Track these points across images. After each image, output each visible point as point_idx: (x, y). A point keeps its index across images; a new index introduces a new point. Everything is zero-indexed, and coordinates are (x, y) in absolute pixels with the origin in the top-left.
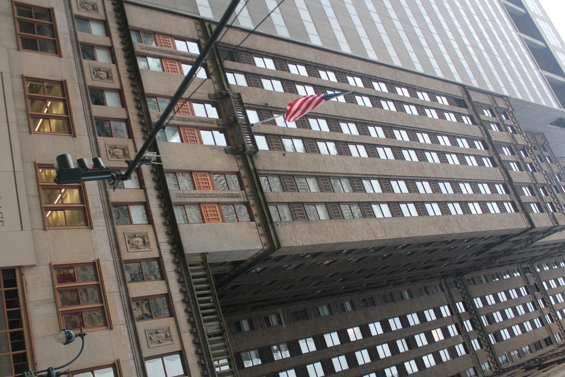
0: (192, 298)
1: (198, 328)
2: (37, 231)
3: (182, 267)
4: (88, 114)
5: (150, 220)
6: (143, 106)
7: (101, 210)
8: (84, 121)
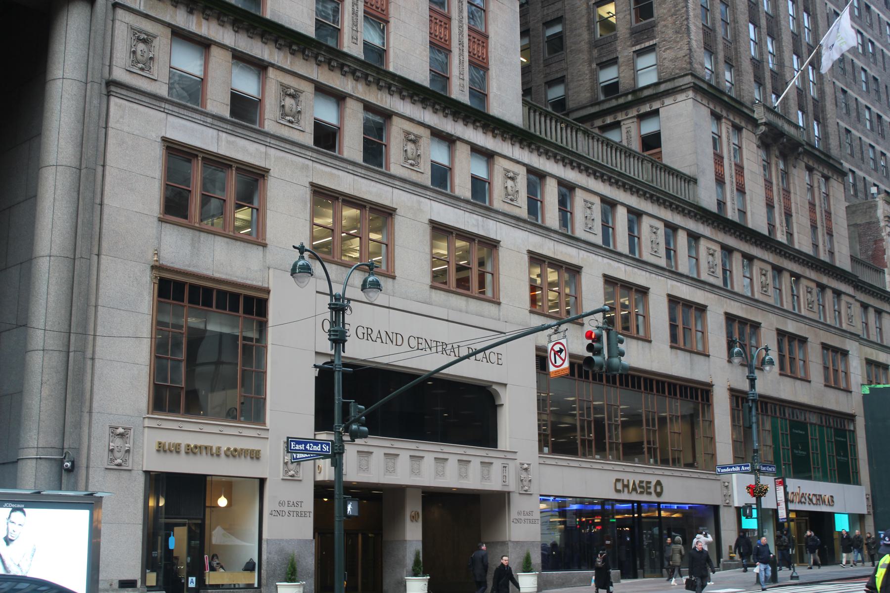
0: (568, 154)
1: (591, 166)
2: (501, 314)
3: (542, 145)
4: (363, 171)
5: (489, 156)
6: (349, 64)
7: (480, 218)
8: (373, 183)
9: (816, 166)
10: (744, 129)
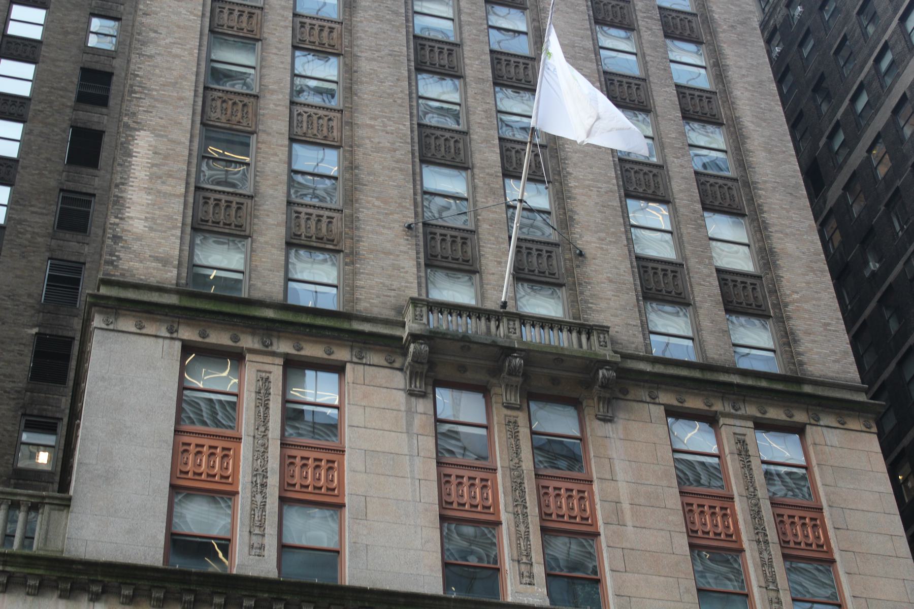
9: (718, 406)
10: (349, 367)
